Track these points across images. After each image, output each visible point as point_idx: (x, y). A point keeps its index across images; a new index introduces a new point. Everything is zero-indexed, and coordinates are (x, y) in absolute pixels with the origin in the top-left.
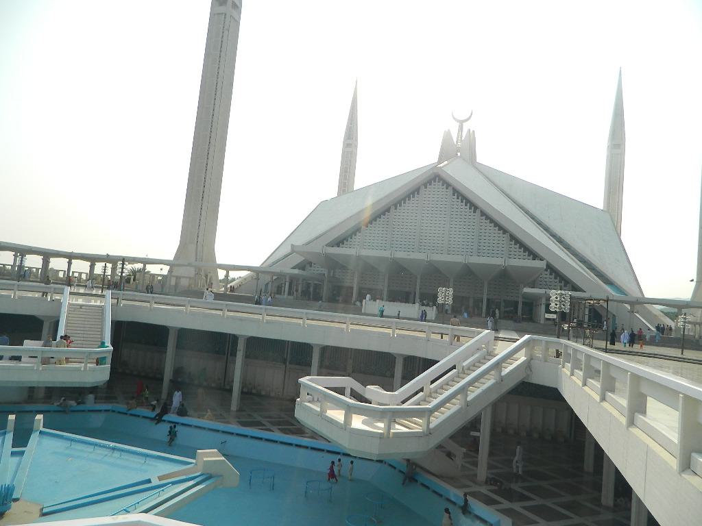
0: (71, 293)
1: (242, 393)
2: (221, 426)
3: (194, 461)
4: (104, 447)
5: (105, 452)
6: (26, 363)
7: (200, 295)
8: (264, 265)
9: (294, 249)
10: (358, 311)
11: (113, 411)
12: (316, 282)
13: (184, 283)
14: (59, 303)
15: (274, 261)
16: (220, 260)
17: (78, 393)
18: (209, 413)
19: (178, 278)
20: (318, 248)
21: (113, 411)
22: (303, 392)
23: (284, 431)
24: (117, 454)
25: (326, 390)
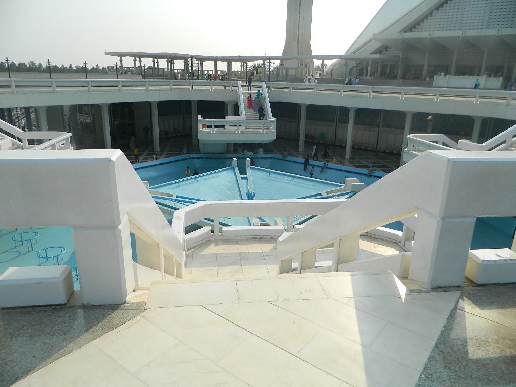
0: (242, 86)
2: (344, 168)
4: (288, 176)
5: (290, 179)
6: (228, 129)
7: (302, 80)
8: (348, 54)
9: (375, 38)
10: (430, 85)
14: (237, 93)
15: (357, 48)
16: (315, 53)
18: (335, 159)
19: (287, 69)
20: (394, 35)
24: (296, 180)
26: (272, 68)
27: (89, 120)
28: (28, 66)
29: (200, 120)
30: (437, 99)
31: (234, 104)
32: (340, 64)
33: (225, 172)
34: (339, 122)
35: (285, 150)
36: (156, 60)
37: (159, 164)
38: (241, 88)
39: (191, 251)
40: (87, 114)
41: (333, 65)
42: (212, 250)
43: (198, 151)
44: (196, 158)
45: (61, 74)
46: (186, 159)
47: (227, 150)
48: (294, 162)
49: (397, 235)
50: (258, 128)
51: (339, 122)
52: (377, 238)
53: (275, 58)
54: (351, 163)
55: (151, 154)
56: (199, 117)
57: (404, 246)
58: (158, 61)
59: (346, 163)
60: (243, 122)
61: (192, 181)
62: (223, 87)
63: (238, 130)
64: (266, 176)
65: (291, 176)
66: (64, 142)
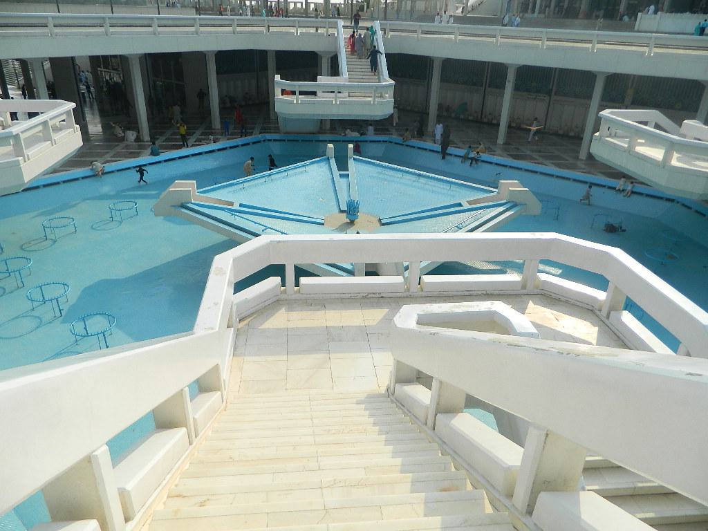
1: (510, 127)
2: (495, 159)
3: (497, 190)
4: (411, 173)
5: (414, 178)
6: (322, 97)
10: (631, 28)
11: (391, 142)
14: (335, 39)
17: (358, 125)
21: (391, 142)
22: (604, 127)
23: (559, 166)
24: (422, 180)
25: (637, 124)
27: (117, 79)
29: (278, 83)
30: (650, 52)
31: (330, 56)
33: (315, 165)
35: (407, 130)
37: (219, 150)
38: (342, 30)
39: (246, 322)
42: (281, 319)
43: (277, 130)
46: (259, 142)
47: (321, 128)
48: (419, 148)
49: (595, 299)
50: (367, 95)
51: (489, 87)
52: (559, 300)
54: (506, 150)
55: (208, 133)
56: (277, 78)
57: (608, 317)
59: (499, 151)
60: (344, 86)
61: (264, 179)
63: (336, 98)
64: (378, 172)
66: (64, 117)
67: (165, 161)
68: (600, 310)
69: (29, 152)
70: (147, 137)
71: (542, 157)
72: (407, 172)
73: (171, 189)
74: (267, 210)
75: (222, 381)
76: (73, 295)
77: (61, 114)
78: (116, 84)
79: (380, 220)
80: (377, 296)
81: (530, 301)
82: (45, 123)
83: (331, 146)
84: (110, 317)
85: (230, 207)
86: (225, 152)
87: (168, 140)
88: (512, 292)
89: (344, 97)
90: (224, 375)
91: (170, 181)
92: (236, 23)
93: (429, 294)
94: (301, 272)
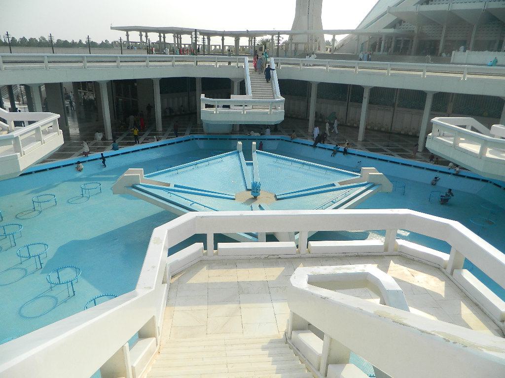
1: (366, 129)
2: (357, 151)
3: (360, 174)
5: (300, 165)
6: (234, 109)
9: (389, 11)
10: (448, 61)
12: (405, 39)
13: (301, 47)
14: (243, 69)
15: (369, 22)
17: (260, 128)
19: (296, 44)
22: (435, 129)
24: (306, 167)
25: (458, 127)
26: (281, 42)
27: (92, 97)
28: (38, 41)
29: (203, 100)
32: (351, 39)
34: (351, 101)
35: (294, 131)
36: (144, 34)
37: (161, 146)
38: (247, 64)
40: (90, 91)
41: (344, 40)
42: (204, 276)
43: (202, 132)
44: (200, 139)
45: (39, 49)
47: (233, 130)
49: (440, 259)
51: (351, 101)
52: (413, 260)
53: (285, 33)
54: (365, 146)
55: (154, 134)
56: (203, 96)
57: (452, 274)
58: (164, 35)
59: (359, 146)
60: (249, 102)
61: (192, 167)
62: (227, 64)
65: (301, 163)
66: (51, 124)
67: (122, 154)
68: (445, 268)
69: (25, 149)
70: (110, 137)
71: (391, 150)
72: (295, 162)
73: (125, 175)
74: (195, 189)
75: (157, 328)
76: (51, 251)
77: (49, 122)
78: (91, 100)
79: (276, 196)
80: (276, 257)
81: (391, 261)
82: (37, 129)
83: (240, 143)
84: (77, 269)
85: (167, 187)
86: (165, 147)
87: (125, 139)
88: (378, 254)
89: (249, 109)
90: (159, 323)
91: (125, 168)
92: (174, 59)
93: (315, 255)
94: (220, 238)
